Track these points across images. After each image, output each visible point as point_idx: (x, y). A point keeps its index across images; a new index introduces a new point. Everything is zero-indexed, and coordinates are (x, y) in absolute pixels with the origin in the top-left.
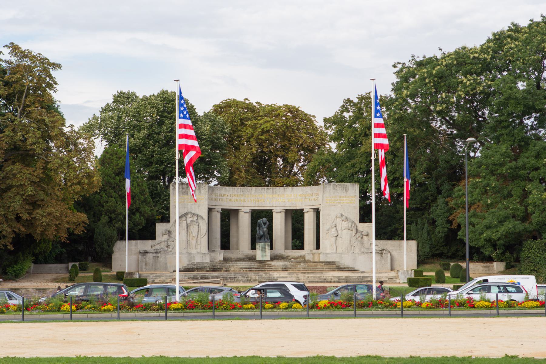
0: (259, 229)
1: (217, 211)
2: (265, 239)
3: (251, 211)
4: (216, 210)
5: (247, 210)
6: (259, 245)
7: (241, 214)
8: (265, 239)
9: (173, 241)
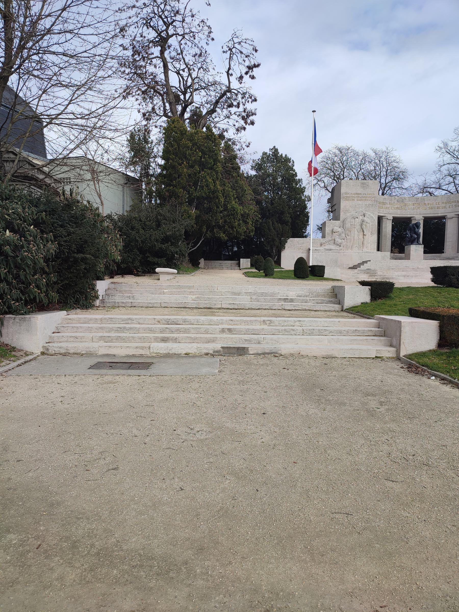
9: (344, 239)
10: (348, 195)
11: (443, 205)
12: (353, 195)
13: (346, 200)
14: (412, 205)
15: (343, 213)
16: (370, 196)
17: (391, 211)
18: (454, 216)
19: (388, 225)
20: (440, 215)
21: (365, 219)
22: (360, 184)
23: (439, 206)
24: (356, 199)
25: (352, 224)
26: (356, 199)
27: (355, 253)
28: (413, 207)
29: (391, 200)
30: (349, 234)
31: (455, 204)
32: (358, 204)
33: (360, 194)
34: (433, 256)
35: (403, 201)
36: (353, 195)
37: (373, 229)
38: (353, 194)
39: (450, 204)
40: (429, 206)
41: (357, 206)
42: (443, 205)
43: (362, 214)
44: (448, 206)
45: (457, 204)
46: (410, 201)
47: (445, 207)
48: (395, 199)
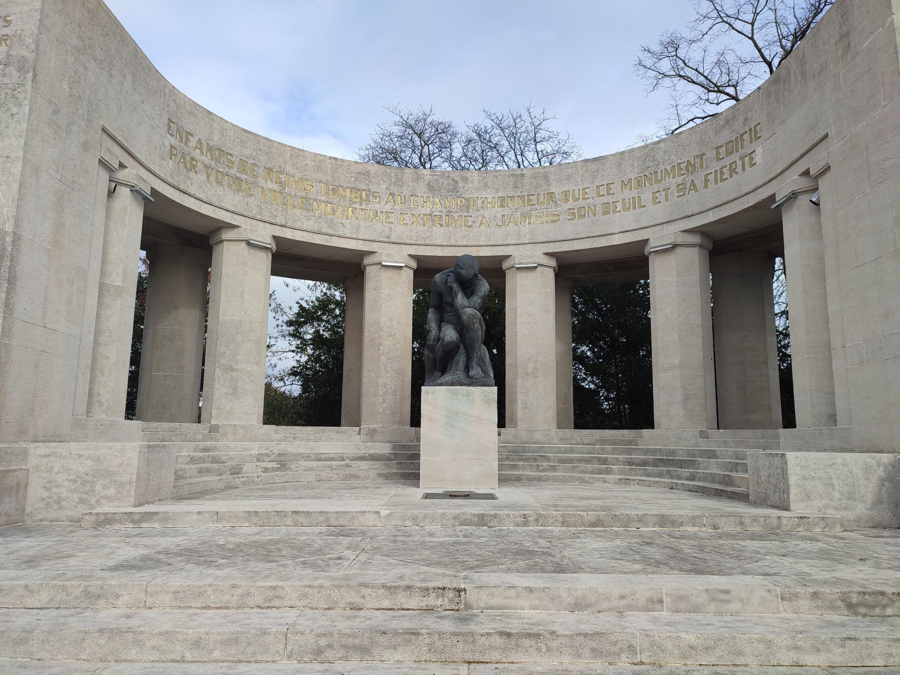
0: (440, 322)
1: (249, 243)
2: (467, 368)
3: (414, 265)
4: (243, 234)
5: (400, 256)
7: (371, 273)
14: (497, 204)
17: (399, 231)
18: (679, 241)
20: (617, 240)
23: (610, 199)
28: (500, 212)
29: (399, 182)
34: (604, 442)
35: (455, 190)
39: (655, 187)
40: (570, 204)
42: (628, 194)
44: (647, 197)
45: (689, 179)
46: (486, 185)
47: (637, 203)
48: (418, 178)
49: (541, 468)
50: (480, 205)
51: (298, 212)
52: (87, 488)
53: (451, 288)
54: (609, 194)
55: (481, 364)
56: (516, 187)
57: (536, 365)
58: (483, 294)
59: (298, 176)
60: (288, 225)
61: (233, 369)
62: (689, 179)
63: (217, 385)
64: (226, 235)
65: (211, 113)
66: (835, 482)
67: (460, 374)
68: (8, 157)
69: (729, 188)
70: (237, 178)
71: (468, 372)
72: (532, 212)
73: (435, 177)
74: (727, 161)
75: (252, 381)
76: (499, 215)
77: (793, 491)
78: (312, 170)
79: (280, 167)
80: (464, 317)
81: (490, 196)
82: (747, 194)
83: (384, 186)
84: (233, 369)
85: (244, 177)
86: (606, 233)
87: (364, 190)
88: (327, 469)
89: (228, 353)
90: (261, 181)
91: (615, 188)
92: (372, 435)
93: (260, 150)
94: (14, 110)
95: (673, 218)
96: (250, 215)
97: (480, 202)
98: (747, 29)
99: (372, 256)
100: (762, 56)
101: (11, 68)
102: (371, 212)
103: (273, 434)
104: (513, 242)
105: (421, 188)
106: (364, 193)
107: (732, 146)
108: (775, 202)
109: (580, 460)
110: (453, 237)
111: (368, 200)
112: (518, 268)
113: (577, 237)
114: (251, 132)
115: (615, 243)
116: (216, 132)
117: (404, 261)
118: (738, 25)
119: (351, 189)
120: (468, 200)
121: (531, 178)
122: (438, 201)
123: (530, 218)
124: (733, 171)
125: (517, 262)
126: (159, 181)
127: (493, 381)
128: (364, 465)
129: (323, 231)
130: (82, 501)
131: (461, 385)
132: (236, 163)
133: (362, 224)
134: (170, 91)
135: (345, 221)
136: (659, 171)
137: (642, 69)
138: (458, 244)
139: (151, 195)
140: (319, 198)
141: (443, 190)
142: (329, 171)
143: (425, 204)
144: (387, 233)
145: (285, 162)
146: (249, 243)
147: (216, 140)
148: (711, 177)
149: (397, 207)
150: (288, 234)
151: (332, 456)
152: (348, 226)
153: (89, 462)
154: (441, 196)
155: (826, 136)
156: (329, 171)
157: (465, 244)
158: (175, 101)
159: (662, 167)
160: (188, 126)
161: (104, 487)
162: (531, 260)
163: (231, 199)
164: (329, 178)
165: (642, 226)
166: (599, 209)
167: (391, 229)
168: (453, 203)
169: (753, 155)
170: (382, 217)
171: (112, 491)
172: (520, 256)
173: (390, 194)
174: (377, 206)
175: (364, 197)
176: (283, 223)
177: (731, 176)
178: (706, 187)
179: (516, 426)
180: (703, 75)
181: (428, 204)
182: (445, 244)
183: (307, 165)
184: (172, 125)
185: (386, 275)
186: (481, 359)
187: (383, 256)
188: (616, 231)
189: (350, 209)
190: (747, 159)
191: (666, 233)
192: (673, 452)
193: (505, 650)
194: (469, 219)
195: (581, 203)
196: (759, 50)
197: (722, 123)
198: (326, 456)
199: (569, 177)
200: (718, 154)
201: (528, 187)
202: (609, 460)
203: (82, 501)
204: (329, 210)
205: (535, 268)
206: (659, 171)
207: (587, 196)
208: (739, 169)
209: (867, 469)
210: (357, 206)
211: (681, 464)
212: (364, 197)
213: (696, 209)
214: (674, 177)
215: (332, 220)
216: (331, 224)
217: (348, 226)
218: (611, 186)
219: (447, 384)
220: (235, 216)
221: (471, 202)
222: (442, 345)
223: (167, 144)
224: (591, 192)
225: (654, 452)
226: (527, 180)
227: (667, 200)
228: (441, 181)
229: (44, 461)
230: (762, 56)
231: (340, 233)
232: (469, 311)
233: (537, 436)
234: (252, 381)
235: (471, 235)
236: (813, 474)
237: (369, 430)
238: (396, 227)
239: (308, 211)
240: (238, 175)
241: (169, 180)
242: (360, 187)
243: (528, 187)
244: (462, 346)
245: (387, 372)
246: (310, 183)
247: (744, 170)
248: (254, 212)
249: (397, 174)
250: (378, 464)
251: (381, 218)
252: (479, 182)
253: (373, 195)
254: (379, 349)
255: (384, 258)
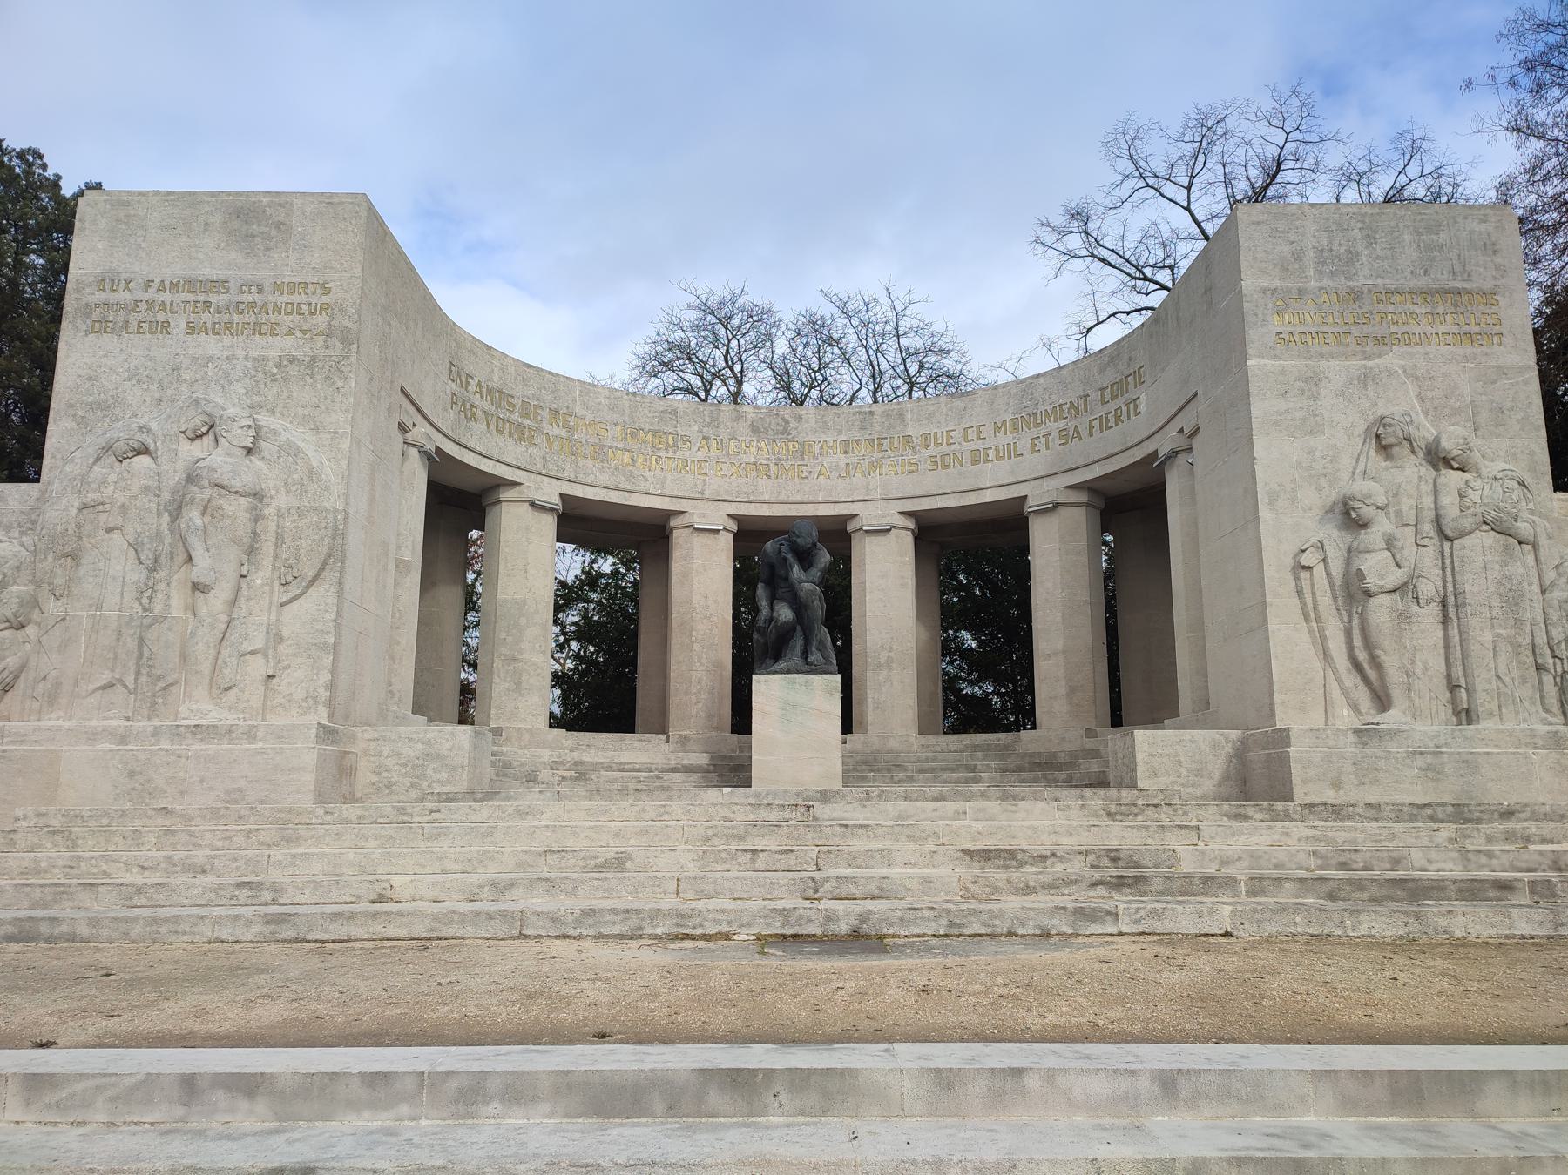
0: (772, 599)
1: (533, 504)
2: (805, 654)
3: (734, 527)
5: (717, 517)
6: (767, 688)
7: (679, 538)
8: (805, 654)
10: (123, 296)
11: (1003, 439)
12: (161, 297)
13: (103, 326)
15: (67, 423)
16: (296, 298)
17: (716, 485)
18: (1062, 498)
19: (697, 563)
20: (989, 497)
21: (220, 459)
22: (217, 219)
23: (980, 445)
24: (179, 323)
25: (91, 497)
26: (179, 323)
27: (93, 736)
28: (842, 460)
29: (715, 422)
30: (59, 581)
31: (1061, 424)
32: (195, 359)
33: (219, 285)
34: (975, 748)
35: (785, 431)
36: (161, 297)
37: (305, 543)
38: (162, 288)
39: (1034, 432)
40: (932, 450)
41: (186, 375)
42: (1003, 439)
43: (197, 422)
44: (1024, 444)
45: (1072, 424)
47: (1012, 451)
48: (739, 418)
49: (896, 779)
50: (817, 451)
51: (590, 463)
52: (418, 772)
53: (785, 559)
54: (979, 438)
55: (821, 648)
56: (863, 428)
57: (892, 654)
58: (823, 565)
59: (589, 417)
60: (578, 479)
61: (515, 660)
62: (1072, 424)
63: (496, 680)
64: (506, 494)
65: (490, 348)
66: (1182, 759)
67: (797, 660)
68: (335, 433)
69: (1113, 439)
70: (520, 425)
71: (806, 658)
72: (884, 460)
73: (760, 415)
74: (1113, 406)
75: (538, 675)
76: (842, 464)
77: (1141, 769)
78: (606, 409)
79: (568, 408)
80: (801, 594)
81: (830, 440)
82: (1133, 447)
83: (696, 428)
84: (515, 660)
85: (526, 422)
86: (976, 487)
87: (670, 433)
88: (633, 781)
89: (510, 639)
90: (546, 428)
91: (985, 432)
92: (684, 744)
93: (544, 388)
94: (340, 384)
95: (1054, 471)
96: (534, 469)
97: (817, 447)
98: (1181, 196)
99: (682, 516)
100: (1203, 232)
101: (334, 339)
102: (680, 461)
103: (564, 741)
104: (861, 498)
105: (743, 429)
106: (670, 437)
107: (1118, 389)
108: (1157, 459)
109: (942, 769)
110: (784, 492)
111: (675, 445)
112: (867, 531)
113: (940, 492)
114: (534, 367)
115: (987, 500)
116: (496, 370)
117: (721, 522)
118: (1169, 189)
119: (655, 432)
120: (802, 444)
121: (882, 417)
122: (764, 446)
123: (881, 467)
124: (1118, 418)
125: (865, 523)
126: (441, 436)
127: (836, 668)
128: (678, 777)
129: (621, 486)
130: (413, 785)
131: (798, 672)
132: (518, 406)
133: (669, 476)
134: (452, 329)
135: (647, 474)
136: (1038, 412)
137: (1040, 248)
138: (790, 500)
139: (436, 453)
140: (615, 445)
141: (770, 432)
142: (627, 411)
143: (747, 450)
144: (700, 487)
145: (574, 401)
146: (533, 504)
147: (496, 380)
148: (1096, 423)
149: (712, 454)
150: (578, 491)
151: (637, 766)
152: (651, 480)
153: (420, 746)
154: (768, 439)
155: (1196, 395)
156: (627, 411)
157: (800, 500)
158: (455, 340)
159: (1041, 408)
160: (469, 368)
161: (436, 770)
162: (884, 521)
163: (513, 451)
164: (627, 419)
165: (1019, 480)
166: (967, 457)
167: (704, 481)
168: (783, 448)
169: (1137, 402)
170: (694, 467)
171: (444, 775)
172: (869, 516)
173: (704, 438)
174: (687, 453)
175: (671, 442)
176: (572, 477)
177: (1116, 425)
178: (1091, 434)
179: (865, 731)
180: (1123, 258)
181: (752, 449)
182: (773, 500)
183: (600, 403)
184: (453, 368)
185: (698, 540)
186: (821, 642)
187: (695, 516)
188: (988, 485)
189: (654, 458)
190: (1132, 406)
191: (1046, 489)
192: (1054, 755)
193: (843, 836)
194: (804, 468)
195: (945, 449)
196: (1199, 225)
197: (1106, 359)
198: (631, 766)
199: (930, 416)
200: (1103, 396)
201: (878, 428)
202: (979, 767)
203: (413, 785)
204: (627, 460)
205: (888, 531)
206: (1038, 412)
207: (952, 441)
208: (1124, 417)
209: (1215, 746)
210: (662, 454)
211: (1060, 766)
212: (671, 442)
213: (1081, 462)
214: (1055, 421)
215: (631, 472)
216: (630, 477)
217: (651, 480)
218: (981, 428)
219: (781, 672)
220: (517, 471)
221: (807, 447)
222: (776, 626)
223: (449, 392)
224: (957, 436)
225: (1032, 755)
226: (877, 419)
227: (1047, 448)
228: (768, 420)
229: (373, 744)
230: (1203, 232)
231: (641, 488)
232: (807, 586)
233: (893, 744)
234: (538, 675)
235: (807, 489)
236: (1160, 752)
237: (680, 736)
238: (710, 479)
239: (602, 461)
240: (520, 420)
241: (450, 433)
242: (666, 429)
243: (878, 428)
244: (798, 628)
245: (702, 664)
246: (603, 426)
247: (1129, 418)
248: (538, 465)
249: (711, 412)
250: (695, 776)
251: (692, 468)
252: (816, 422)
253: (682, 439)
254: (691, 635)
255: (696, 519)
